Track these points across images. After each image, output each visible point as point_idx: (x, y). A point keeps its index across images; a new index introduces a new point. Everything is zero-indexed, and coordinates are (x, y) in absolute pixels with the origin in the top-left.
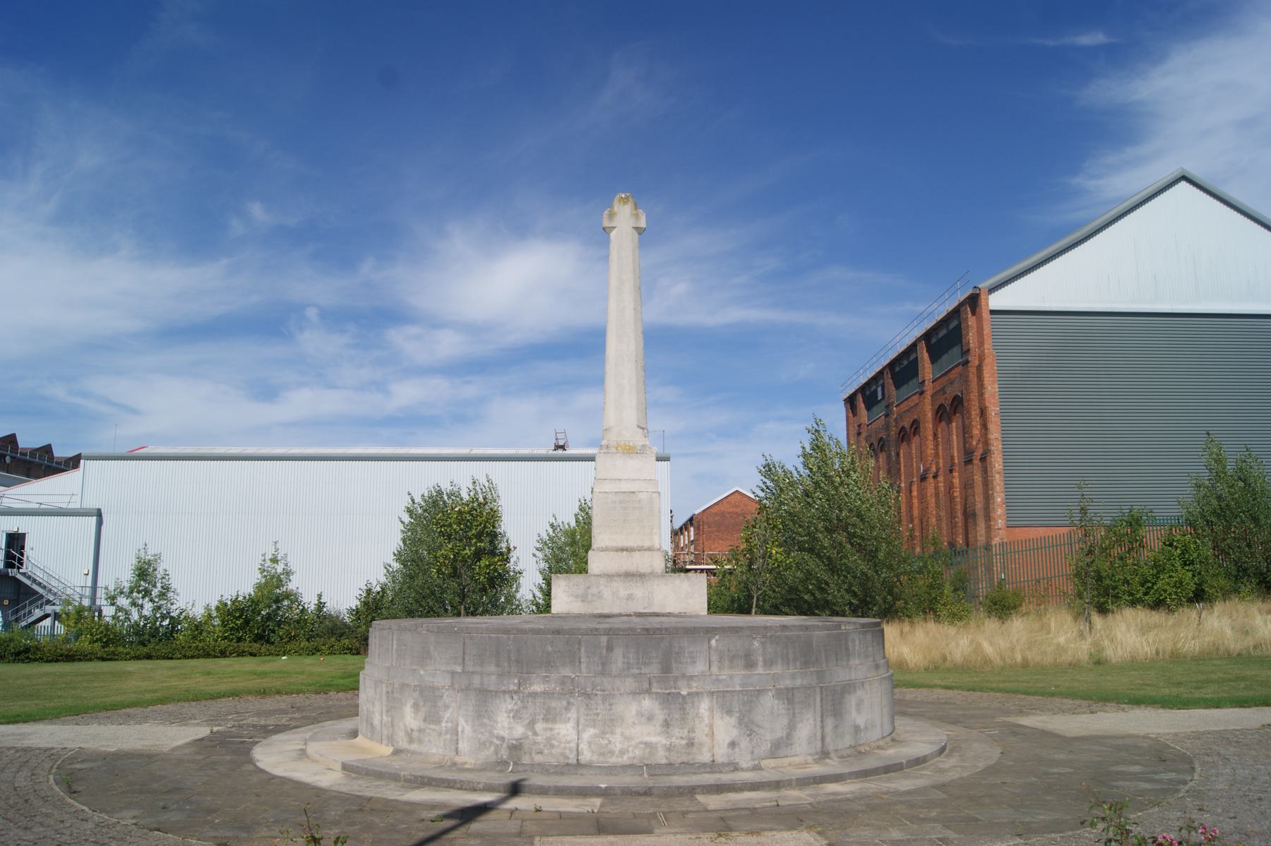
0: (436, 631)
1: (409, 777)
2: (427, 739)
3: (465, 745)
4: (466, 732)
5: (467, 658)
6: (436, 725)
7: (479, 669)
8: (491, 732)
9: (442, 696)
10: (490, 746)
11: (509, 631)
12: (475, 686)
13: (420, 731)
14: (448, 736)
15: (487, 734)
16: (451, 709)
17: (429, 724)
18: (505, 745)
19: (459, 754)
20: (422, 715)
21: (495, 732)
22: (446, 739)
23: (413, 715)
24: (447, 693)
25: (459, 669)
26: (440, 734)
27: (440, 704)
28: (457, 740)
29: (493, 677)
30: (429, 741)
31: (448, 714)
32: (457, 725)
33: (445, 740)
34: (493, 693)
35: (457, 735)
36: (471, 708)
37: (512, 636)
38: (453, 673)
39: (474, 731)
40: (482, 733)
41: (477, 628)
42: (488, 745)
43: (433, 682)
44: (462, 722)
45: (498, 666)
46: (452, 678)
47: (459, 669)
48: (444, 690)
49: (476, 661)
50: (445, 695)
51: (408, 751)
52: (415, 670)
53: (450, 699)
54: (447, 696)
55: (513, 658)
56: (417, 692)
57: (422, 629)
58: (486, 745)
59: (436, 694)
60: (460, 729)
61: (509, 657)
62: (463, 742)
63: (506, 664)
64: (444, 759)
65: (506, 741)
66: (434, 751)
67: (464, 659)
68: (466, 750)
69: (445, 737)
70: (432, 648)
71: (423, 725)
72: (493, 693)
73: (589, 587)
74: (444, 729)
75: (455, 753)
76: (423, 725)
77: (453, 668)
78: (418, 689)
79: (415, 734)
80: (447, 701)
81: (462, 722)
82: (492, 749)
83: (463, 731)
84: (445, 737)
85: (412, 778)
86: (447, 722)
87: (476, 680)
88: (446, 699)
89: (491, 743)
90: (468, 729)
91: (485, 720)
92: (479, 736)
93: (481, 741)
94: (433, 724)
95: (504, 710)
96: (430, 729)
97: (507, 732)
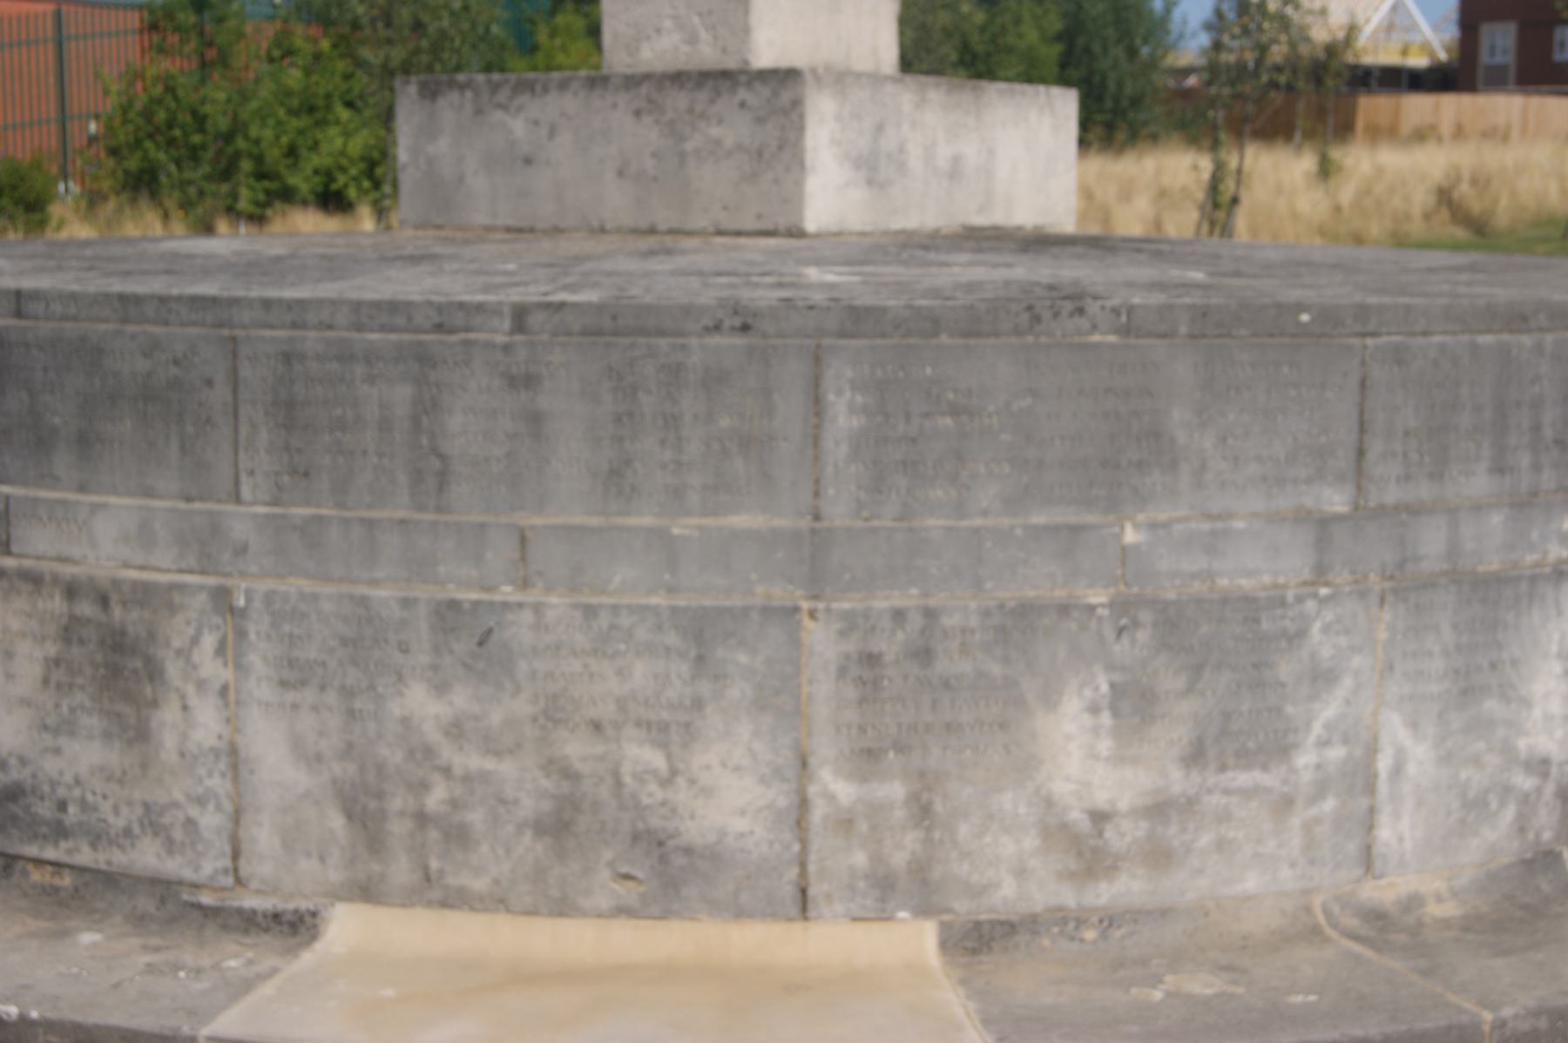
0: (1183, 330)
1: (1525, 1026)
2: (1205, 840)
3: (1405, 825)
4: (1411, 769)
5: (1376, 447)
6: (1265, 768)
7: (1424, 491)
8: (1507, 750)
9: (1302, 634)
10: (1502, 804)
11: (1525, 319)
12: (1426, 566)
13: (1159, 809)
14: (1329, 805)
15: (1492, 760)
16: (1348, 682)
17: (1223, 768)
18: (1550, 789)
19: (1378, 866)
20: (1173, 734)
21: (1522, 744)
22: (1317, 821)
23: (1105, 746)
24: (1329, 615)
25: (1336, 500)
26: (1286, 804)
27: (1286, 669)
28: (1372, 811)
29: (1496, 519)
30: (1221, 845)
31: (1329, 710)
32: (1372, 750)
33: (1308, 827)
34: (1524, 587)
35: (1370, 788)
36: (1437, 665)
37: (1549, 338)
38: (1324, 524)
39: (1446, 759)
40: (1476, 761)
41: (1408, 309)
42: (1494, 805)
43: (1210, 576)
44: (1394, 729)
45: (1499, 469)
46: (1322, 543)
47: (1336, 500)
48: (1311, 605)
49: (1414, 457)
50: (1316, 627)
51: (1067, 921)
52: (1076, 530)
53: (1343, 641)
54: (1326, 629)
55: (1548, 433)
56: (1142, 636)
57: (1083, 323)
58: (1486, 804)
59: (1265, 625)
60: (1384, 764)
61: (1536, 428)
62: (1397, 816)
63: (1525, 460)
64: (1308, 910)
65: (1554, 770)
66: (1252, 883)
67: (1361, 453)
68: (1408, 845)
69: (1313, 812)
70: (1178, 417)
71: (1178, 781)
72: (1524, 587)
73: (880, 128)
74: (1307, 777)
75: (1359, 872)
76: (1178, 781)
77: (1309, 502)
78: (1146, 616)
79: (1123, 835)
80: (1326, 652)
81: (1394, 729)
82: (1509, 813)
83: (1397, 770)
84: (1313, 812)
85: (1543, 1024)
86: (1324, 743)
87: (1431, 541)
88: (1321, 643)
89: (1507, 790)
90: (1421, 756)
91: (1491, 706)
92: (1463, 775)
93: (1471, 794)
94: (1248, 767)
95: (1554, 648)
96: (1227, 792)
97: (1559, 734)
